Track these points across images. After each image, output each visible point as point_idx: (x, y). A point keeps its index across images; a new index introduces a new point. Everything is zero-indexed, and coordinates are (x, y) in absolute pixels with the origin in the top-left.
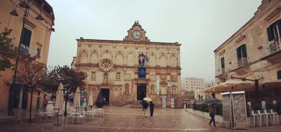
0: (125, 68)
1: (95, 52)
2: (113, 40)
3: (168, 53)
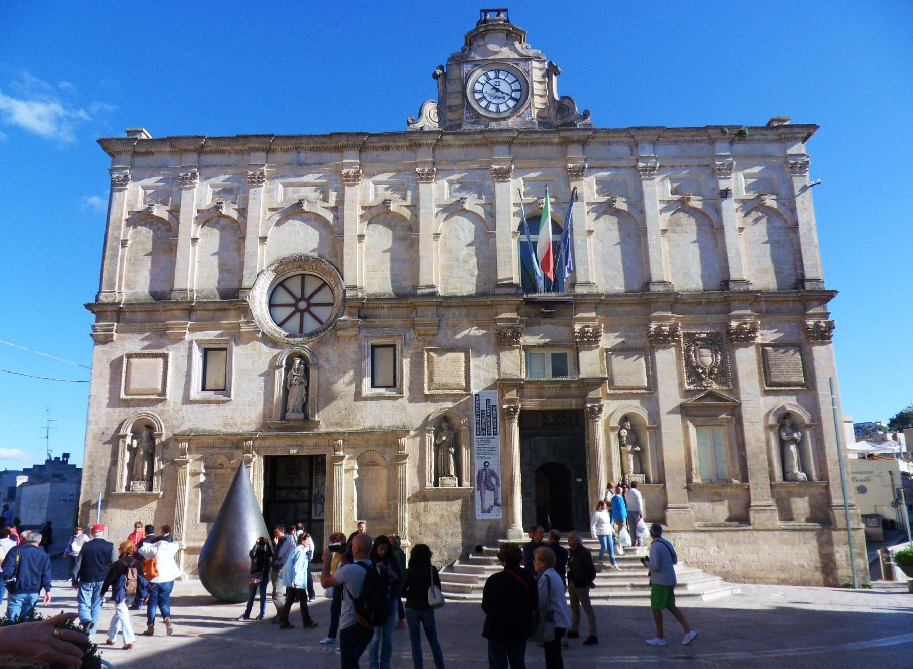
3: (726, 193)
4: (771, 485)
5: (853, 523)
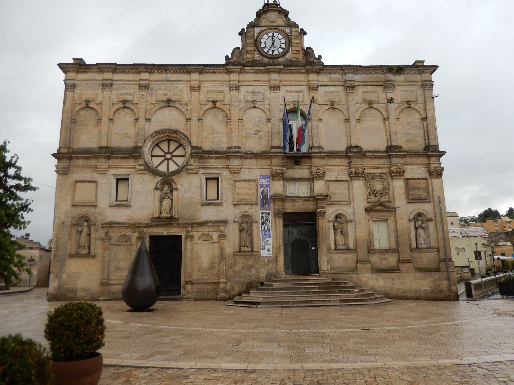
0: (236, 157)
1: (127, 105)
3: (391, 100)
4: (411, 250)
5: (451, 269)
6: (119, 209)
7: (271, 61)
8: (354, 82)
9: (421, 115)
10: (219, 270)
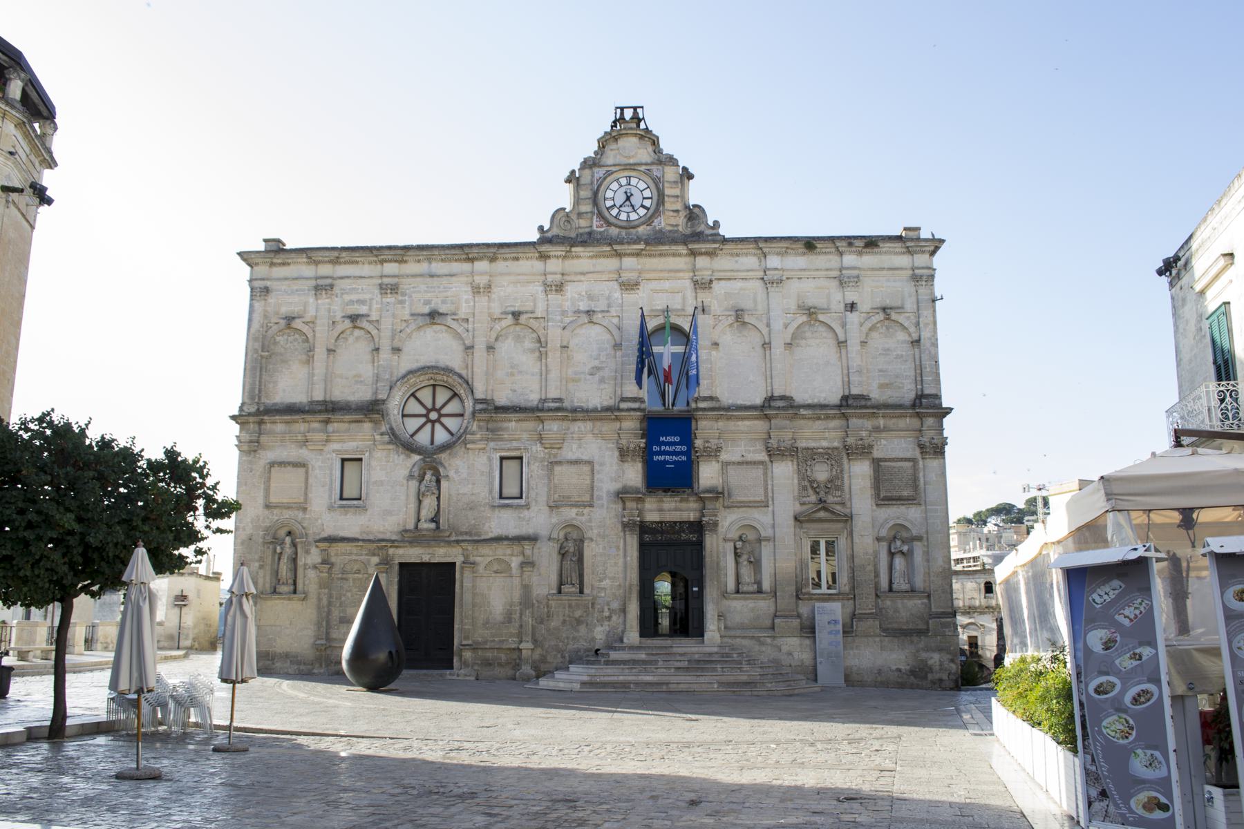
2: (470, 246)
3: (852, 307)
4: (877, 595)
6: (346, 515)
7: (623, 233)
8: (781, 272)
9: (910, 335)
10: (521, 626)
